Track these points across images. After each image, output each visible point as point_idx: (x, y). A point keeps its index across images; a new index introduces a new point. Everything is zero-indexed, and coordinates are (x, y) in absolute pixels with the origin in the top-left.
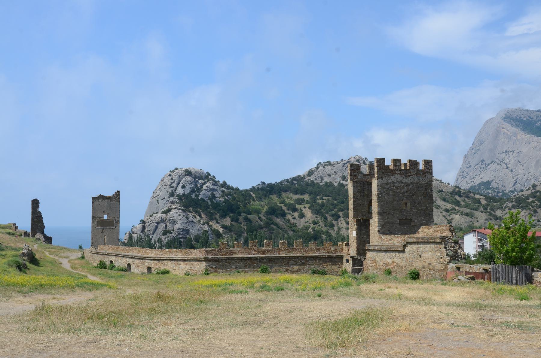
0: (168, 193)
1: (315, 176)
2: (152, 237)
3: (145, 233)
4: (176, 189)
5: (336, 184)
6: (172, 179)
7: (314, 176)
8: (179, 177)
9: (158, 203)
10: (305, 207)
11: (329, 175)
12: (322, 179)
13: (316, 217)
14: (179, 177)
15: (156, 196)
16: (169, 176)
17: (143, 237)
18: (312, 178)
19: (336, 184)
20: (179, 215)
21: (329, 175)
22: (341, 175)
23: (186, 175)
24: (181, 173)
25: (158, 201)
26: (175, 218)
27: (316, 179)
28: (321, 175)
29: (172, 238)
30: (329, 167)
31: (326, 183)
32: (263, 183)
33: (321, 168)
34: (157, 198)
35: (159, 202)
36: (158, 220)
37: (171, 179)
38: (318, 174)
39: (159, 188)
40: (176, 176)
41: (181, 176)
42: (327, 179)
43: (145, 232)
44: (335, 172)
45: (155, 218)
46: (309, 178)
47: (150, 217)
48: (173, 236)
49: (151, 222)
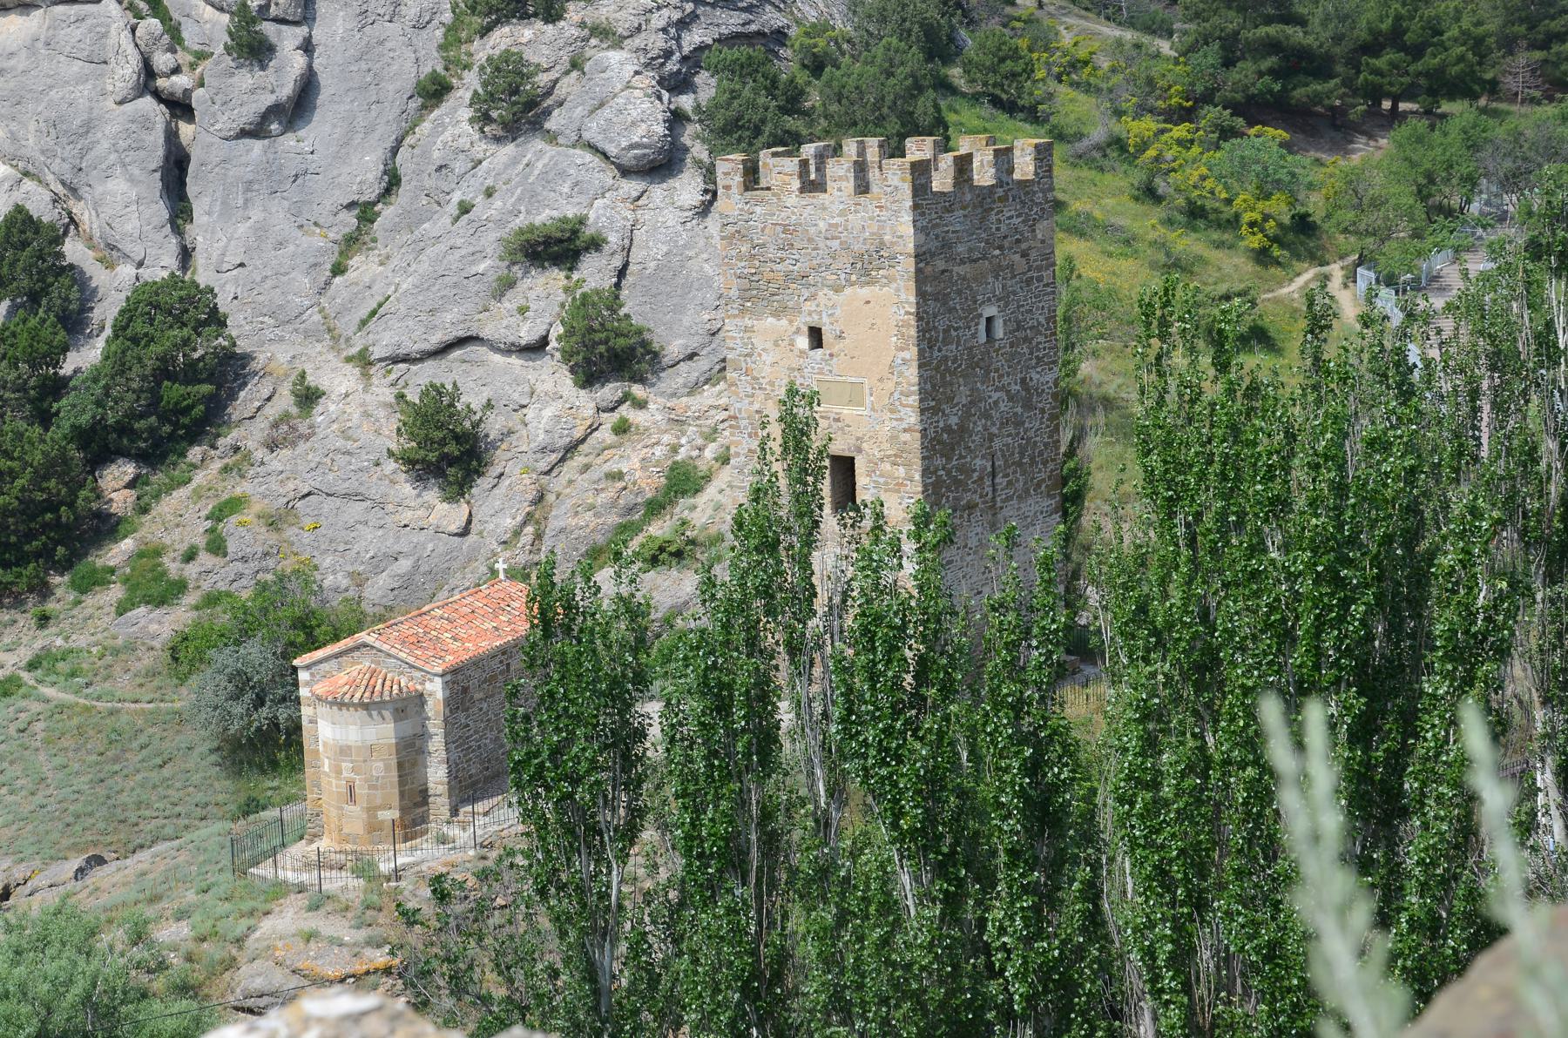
2: (307, 47)
17: (162, 61)
29: (668, 54)
48: (658, 20)
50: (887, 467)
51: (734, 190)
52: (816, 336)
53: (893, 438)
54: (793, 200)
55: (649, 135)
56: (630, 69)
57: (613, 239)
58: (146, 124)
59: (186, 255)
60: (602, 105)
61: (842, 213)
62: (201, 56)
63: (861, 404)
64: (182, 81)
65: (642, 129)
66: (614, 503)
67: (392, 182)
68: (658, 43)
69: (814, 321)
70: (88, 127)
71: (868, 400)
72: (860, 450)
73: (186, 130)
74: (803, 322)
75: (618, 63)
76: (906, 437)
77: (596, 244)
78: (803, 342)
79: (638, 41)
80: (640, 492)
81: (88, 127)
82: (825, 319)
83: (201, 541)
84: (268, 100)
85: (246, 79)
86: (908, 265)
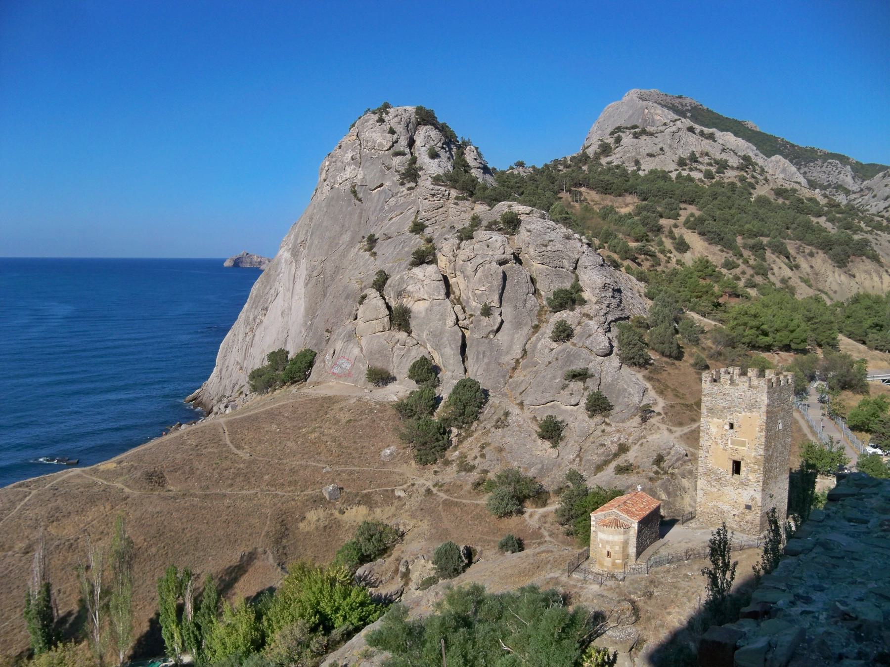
0: (393, 170)
1: (620, 156)
3: (459, 301)
4: (414, 160)
5: (673, 175)
6: (392, 131)
7: (618, 156)
8: (407, 126)
9: (360, 200)
10: (676, 226)
11: (650, 155)
12: (637, 163)
13: (723, 251)
14: (407, 126)
15: (344, 179)
16: (378, 121)
17: (461, 317)
18: (615, 159)
19: (673, 175)
20: (568, 238)
21: (650, 155)
22: (676, 158)
23: (419, 124)
24: (406, 116)
25: (354, 193)
26: (561, 247)
27: (623, 163)
28: (634, 154)
30: (644, 137)
31: (652, 172)
32: (521, 164)
33: (627, 139)
34: (348, 185)
35: (360, 195)
36: (504, 253)
37: (389, 133)
38: (625, 152)
39: (349, 158)
40: (399, 123)
41: (411, 126)
42: (648, 166)
43: (454, 293)
44: (661, 149)
45: (488, 246)
46: (609, 159)
47: (461, 240)
48: (602, 312)
49: (479, 260)
50: (752, 465)
51: (708, 382)
52: (732, 426)
53: (755, 457)
54: (727, 387)
55: (605, 346)
56: (596, 327)
57: (596, 375)
58: (456, 333)
59: (466, 371)
60: (590, 336)
61: (744, 392)
62: (471, 315)
63: (745, 446)
64: (466, 322)
65: (603, 345)
66: (603, 453)
67: (525, 352)
68: (603, 319)
69: (731, 421)
70: (441, 333)
71: (747, 445)
72: (743, 459)
73: (468, 334)
74: (727, 421)
75: (593, 324)
76: (759, 457)
77: (592, 376)
78: (727, 427)
79: (596, 318)
80: (611, 450)
81: (441, 333)
82: (735, 421)
83: (478, 455)
84: (491, 329)
85: (485, 320)
86: (764, 408)
